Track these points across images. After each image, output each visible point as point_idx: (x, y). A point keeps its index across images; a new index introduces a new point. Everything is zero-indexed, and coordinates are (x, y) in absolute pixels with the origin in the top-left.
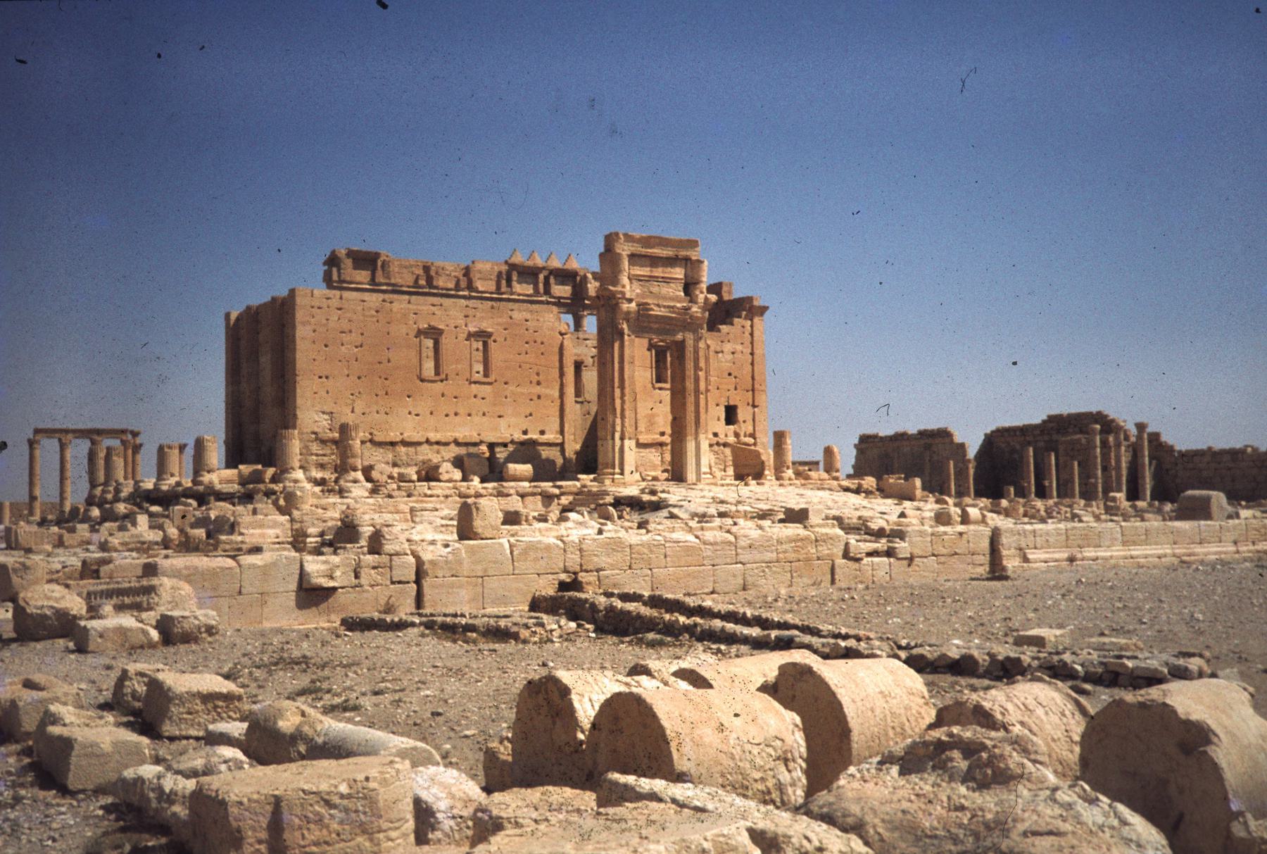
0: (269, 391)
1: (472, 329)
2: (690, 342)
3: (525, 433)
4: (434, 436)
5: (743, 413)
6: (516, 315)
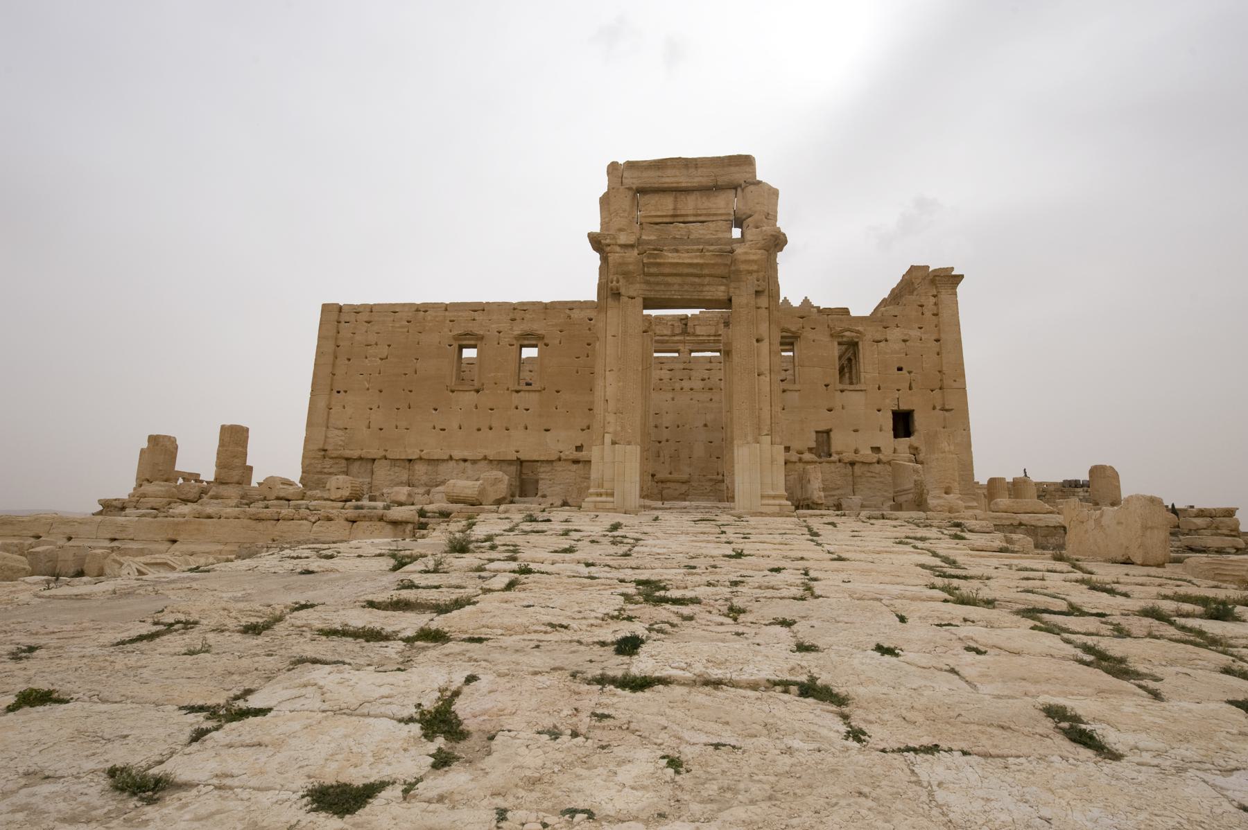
1: (517, 332)
3: (579, 448)
4: (457, 454)
5: (919, 421)
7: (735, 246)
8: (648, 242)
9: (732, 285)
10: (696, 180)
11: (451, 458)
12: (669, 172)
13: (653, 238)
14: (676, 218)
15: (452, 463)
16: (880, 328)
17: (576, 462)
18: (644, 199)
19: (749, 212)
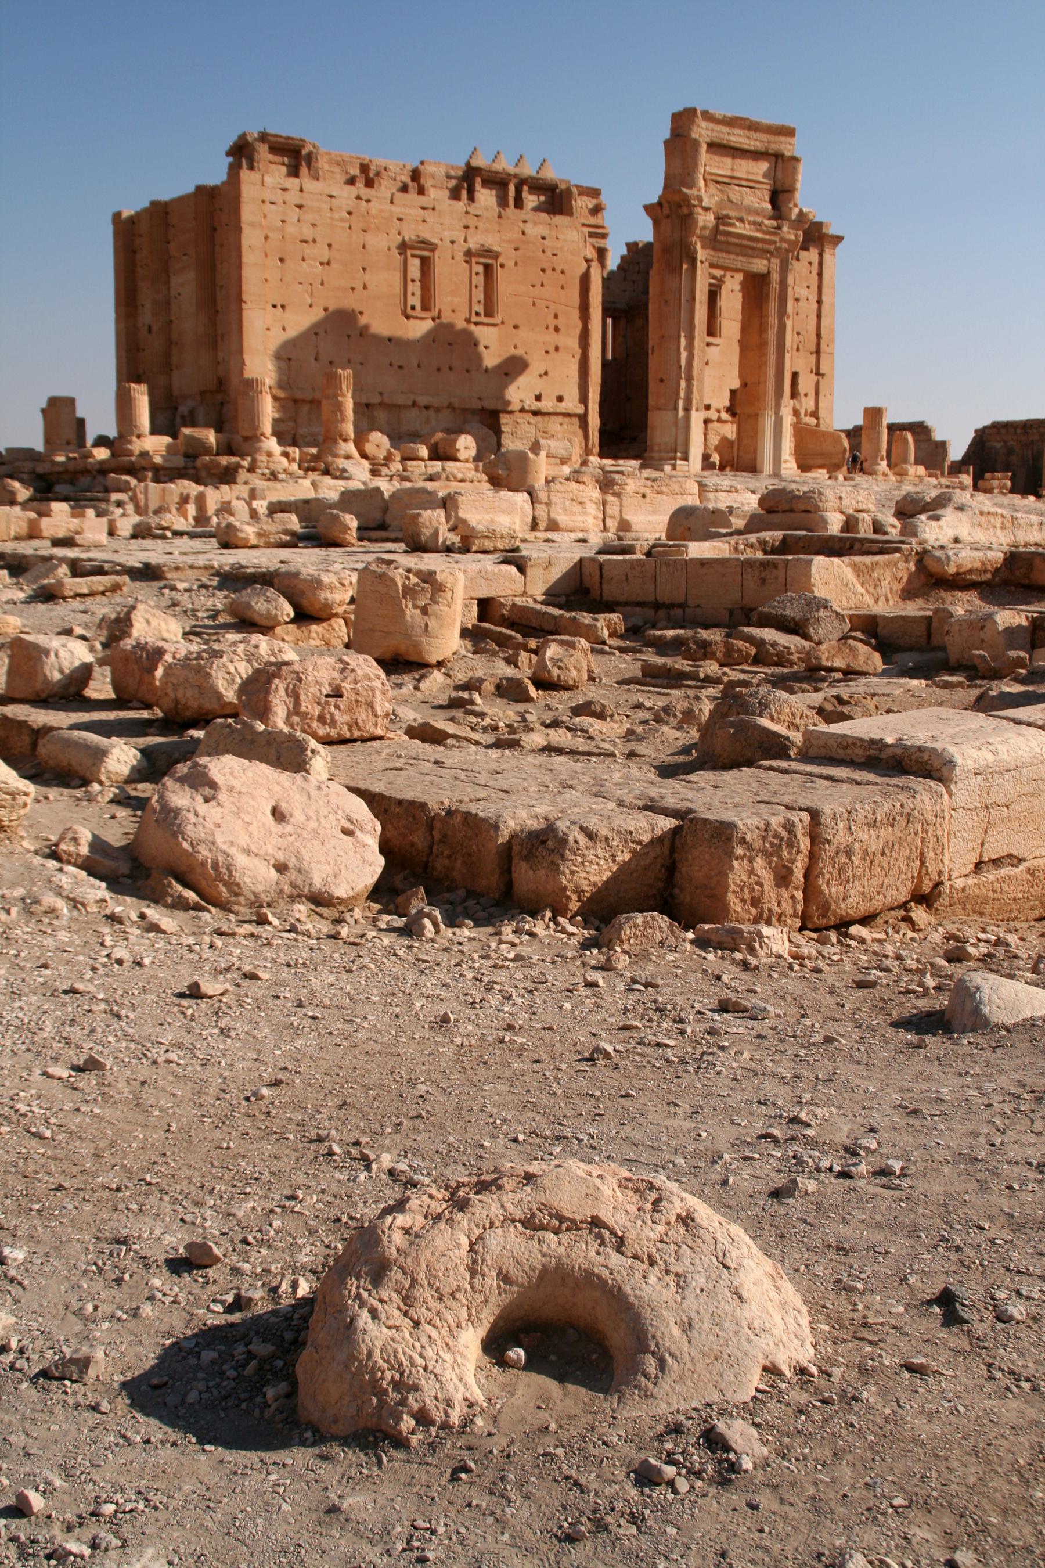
0: (189, 323)
1: (473, 245)
2: (775, 277)
3: (538, 398)
4: (422, 400)
6: (529, 228)
11: (414, 404)
12: (737, 131)
14: (732, 181)
15: (415, 411)
17: (536, 413)
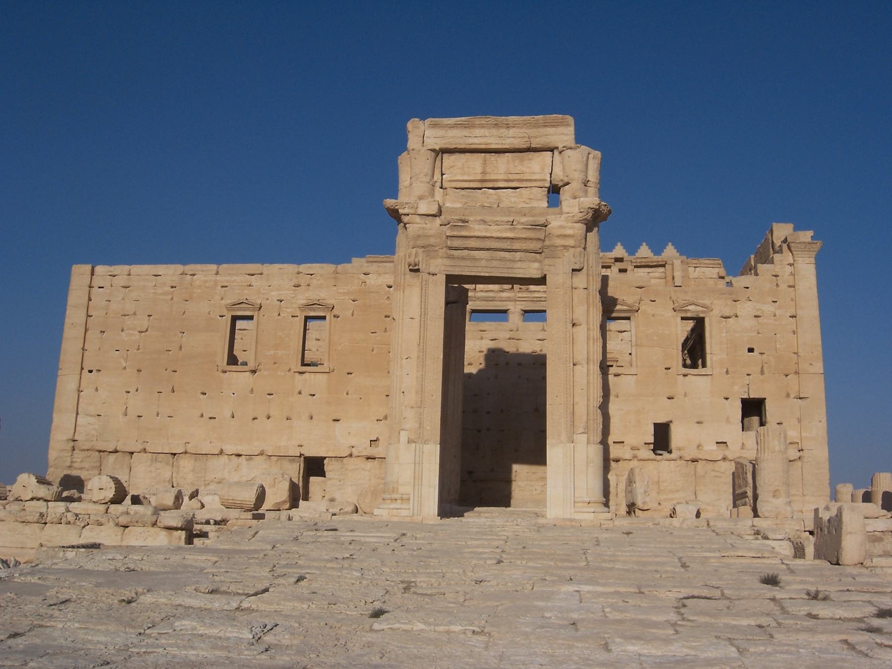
4: (230, 449)
7: (550, 218)
8: (453, 211)
9: (547, 261)
10: (508, 141)
11: (221, 452)
12: (478, 132)
13: (458, 205)
14: (484, 184)
15: (224, 459)
16: (730, 302)
18: (448, 159)
19: (566, 180)
